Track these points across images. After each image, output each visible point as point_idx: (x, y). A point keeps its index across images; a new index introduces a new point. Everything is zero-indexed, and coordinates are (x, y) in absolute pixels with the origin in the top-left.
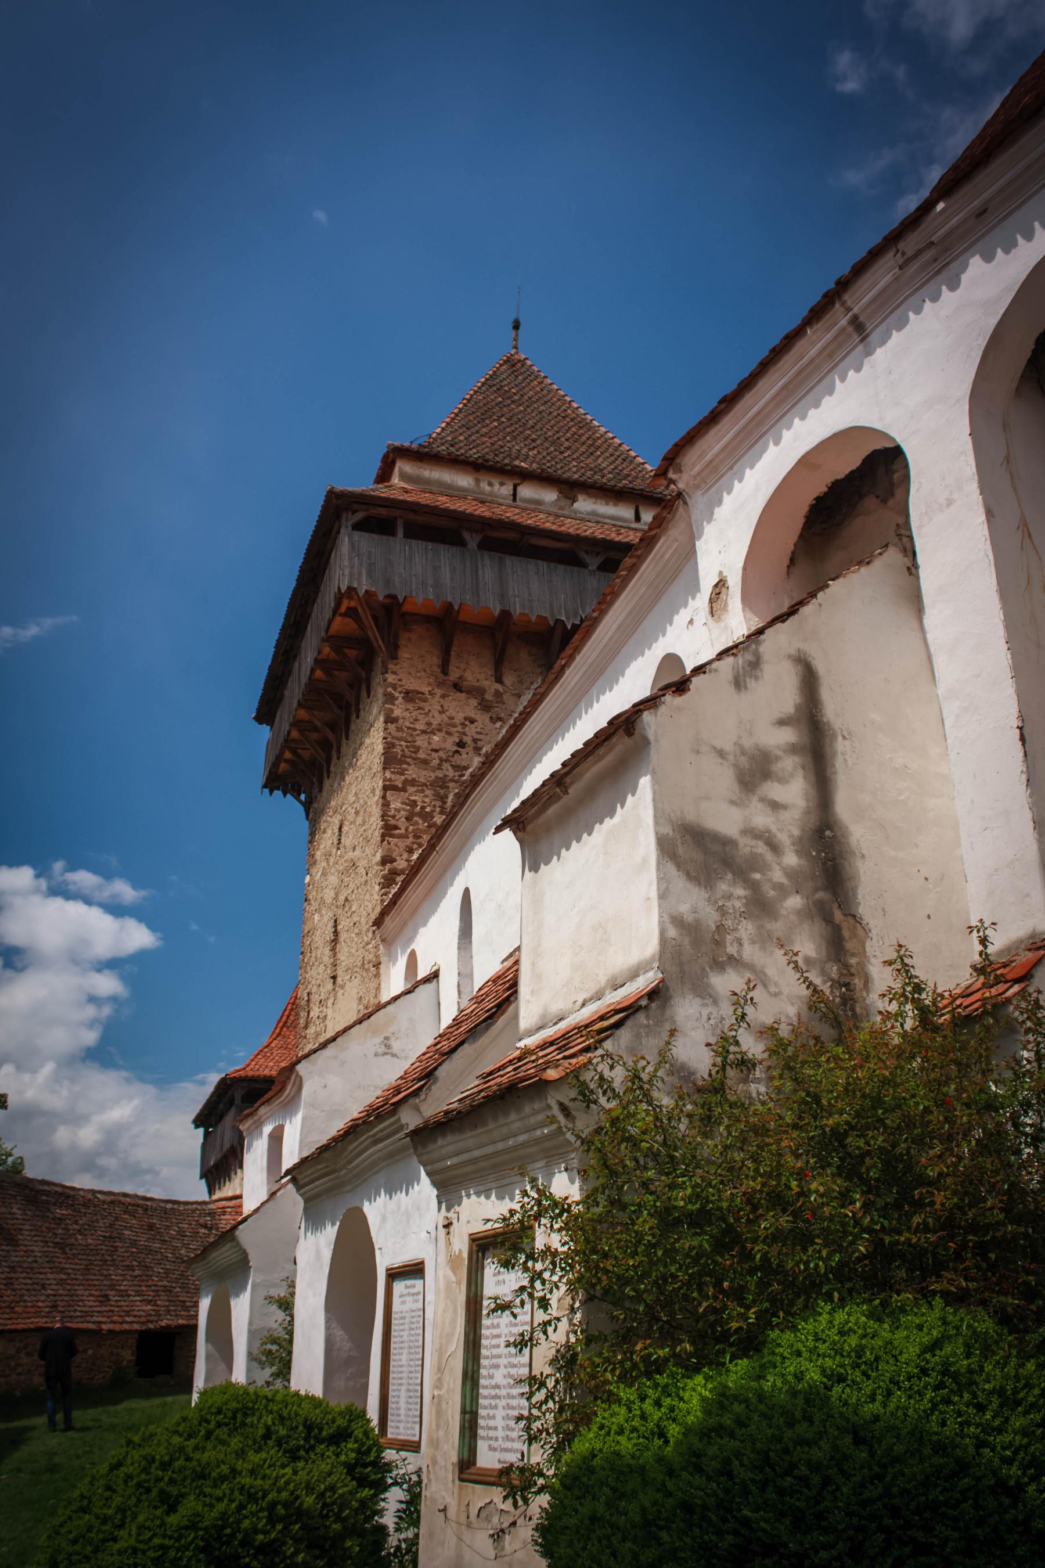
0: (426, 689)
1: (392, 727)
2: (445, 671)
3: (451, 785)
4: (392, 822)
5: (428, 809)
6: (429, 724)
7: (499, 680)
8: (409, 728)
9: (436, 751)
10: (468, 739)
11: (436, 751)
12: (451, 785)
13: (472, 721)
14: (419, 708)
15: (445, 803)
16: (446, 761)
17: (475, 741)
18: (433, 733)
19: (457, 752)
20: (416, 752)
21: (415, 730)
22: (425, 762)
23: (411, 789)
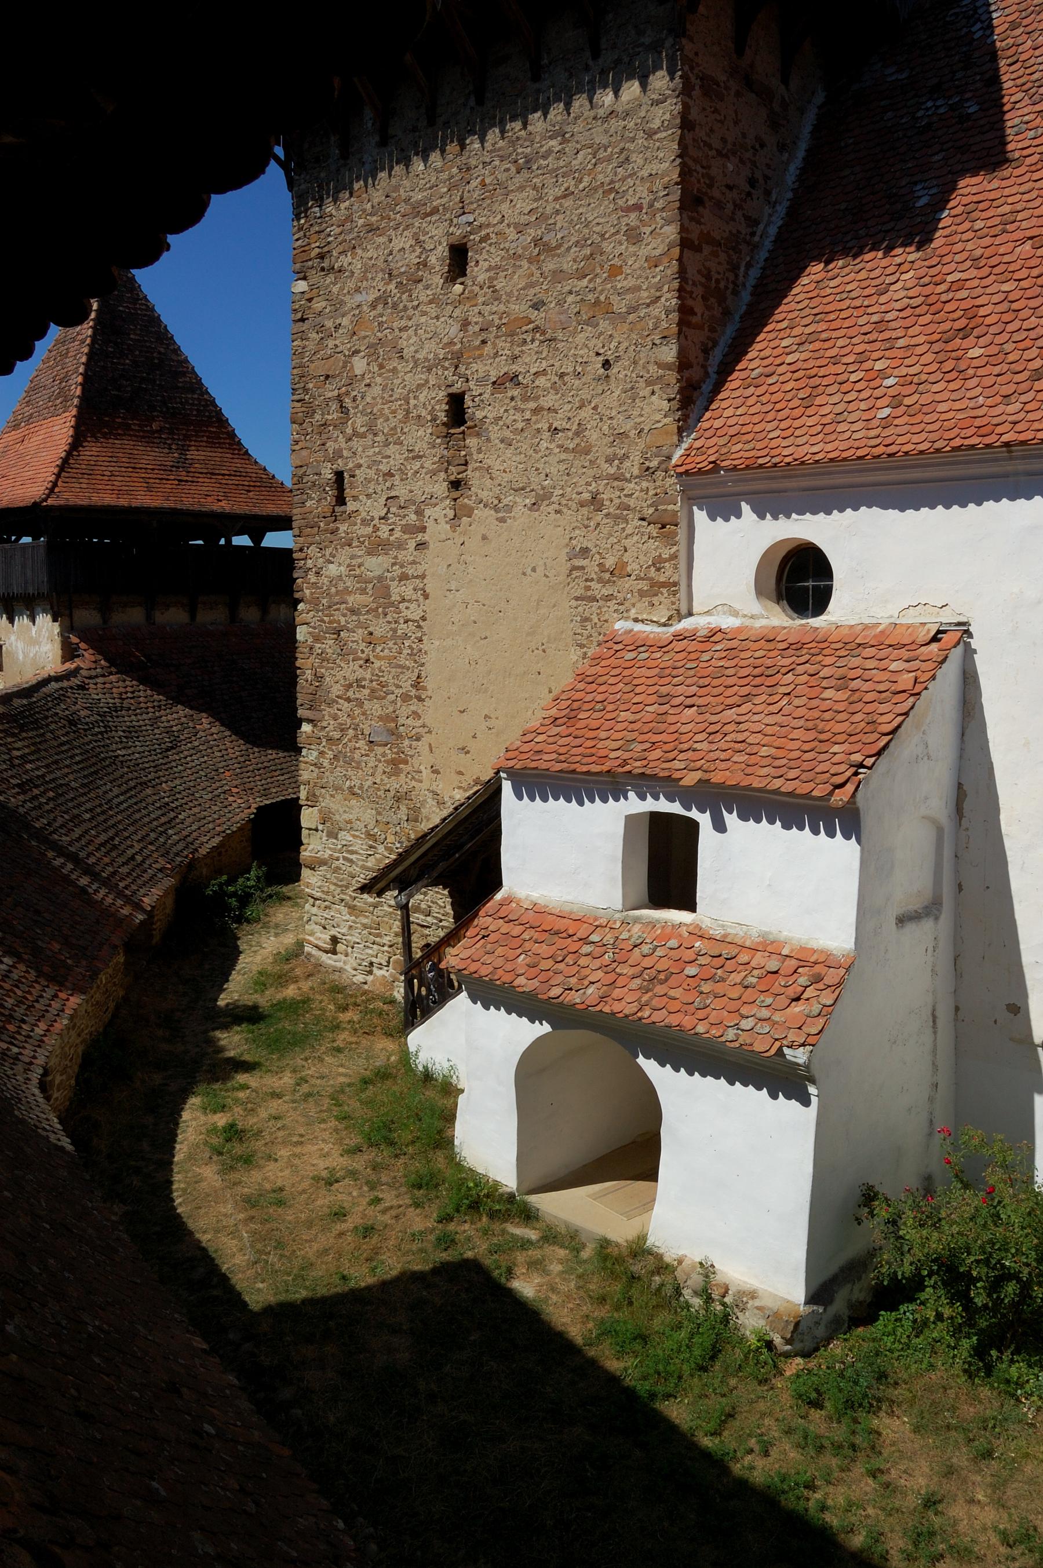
0: (722, 78)
1: (689, 136)
2: (740, 51)
3: (744, 247)
4: (690, 302)
5: (722, 285)
6: (724, 140)
7: (785, 81)
8: (705, 143)
9: (730, 188)
10: (758, 175)
11: (730, 188)
12: (744, 247)
13: (762, 146)
14: (716, 111)
15: (737, 276)
16: (741, 208)
17: (766, 178)
18: (726, 156)
19: (749, 194)
20: (710, 186)
21: (711, 148)
22: (719, 205)
23: (707, 249)
